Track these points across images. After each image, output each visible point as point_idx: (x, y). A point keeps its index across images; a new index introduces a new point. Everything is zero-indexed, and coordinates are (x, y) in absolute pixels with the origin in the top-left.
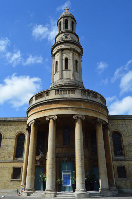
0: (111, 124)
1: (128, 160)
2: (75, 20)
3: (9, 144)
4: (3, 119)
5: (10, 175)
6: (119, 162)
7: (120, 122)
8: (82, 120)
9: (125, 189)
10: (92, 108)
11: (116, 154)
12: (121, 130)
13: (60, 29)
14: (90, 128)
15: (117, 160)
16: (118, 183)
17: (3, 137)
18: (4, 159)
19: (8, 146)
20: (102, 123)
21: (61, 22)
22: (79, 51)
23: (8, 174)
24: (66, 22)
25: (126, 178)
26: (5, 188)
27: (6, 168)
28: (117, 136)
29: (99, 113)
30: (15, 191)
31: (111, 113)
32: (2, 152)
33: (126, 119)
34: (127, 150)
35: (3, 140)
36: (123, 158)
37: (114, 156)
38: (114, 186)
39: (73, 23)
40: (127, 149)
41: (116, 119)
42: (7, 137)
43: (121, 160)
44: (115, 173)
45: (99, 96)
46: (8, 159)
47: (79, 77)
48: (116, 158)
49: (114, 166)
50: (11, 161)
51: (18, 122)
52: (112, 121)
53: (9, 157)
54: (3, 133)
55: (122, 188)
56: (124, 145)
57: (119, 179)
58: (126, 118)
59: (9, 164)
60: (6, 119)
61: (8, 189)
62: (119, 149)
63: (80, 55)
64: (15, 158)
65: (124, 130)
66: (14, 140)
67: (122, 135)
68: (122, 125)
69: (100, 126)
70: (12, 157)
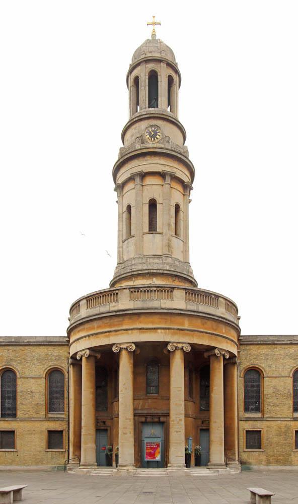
0: (246, 352)
1: (267, 419)
2: (177, 72)
3: (33, 389)
4: (13, 340)
5: (44, 443)
6: (251, 423)
7: (264, 350)
8: (184, 351)
9: (256, 465)
10: (206, 329)
11: (246, 409)
12: (263, 365)
13: (134, 109)
14: (199, 363)
15: (247, 419)
16: (245, 456)
17: (18, 376)
18: (27, 416)
19: (31, 392)
20: (224, 356)
21: (136, 80)
22: (183, 174)
23: (40, 441)
24: (153, 77)
25: (260, 449)
26: (37, 464)
27: (34, 430)
28: (254, 375)
29: (218, 337)
30: (55, 467)
31: (246, 330)
32: (22, 404)
33: (276, 344)
34: (269, 403)
35: (19, 382)
36: (259, 415)
37: (242, 413)
38: (235, 460)
39: (170, 80)
40: (269, 400)
41: (256, 343)
42: (27, 375)
43: (255, 420)
44: (240, 440)
45: (224, 301)
46: (35, 416)
47: (182, 250)
48: (247, 415)
49: (240, 429)
50: (42, 419)
51: (48, 345)
52: (248, 347)
53: (37, 413)
54: (17, 368)
55: (250, 464)
56: (265, 393)
57: (247, 450)
58: (278, 341)
59: (38, 425)
60: (18, 340)
61: (42, 464)
62: (254, 400)
63: (187, 187)
64: (50, 415)
65: (270, 366)
66: (42, 382)
67: (265, 376)
68: (268, 355)
69: (220, 362)
70: (44, 413)
